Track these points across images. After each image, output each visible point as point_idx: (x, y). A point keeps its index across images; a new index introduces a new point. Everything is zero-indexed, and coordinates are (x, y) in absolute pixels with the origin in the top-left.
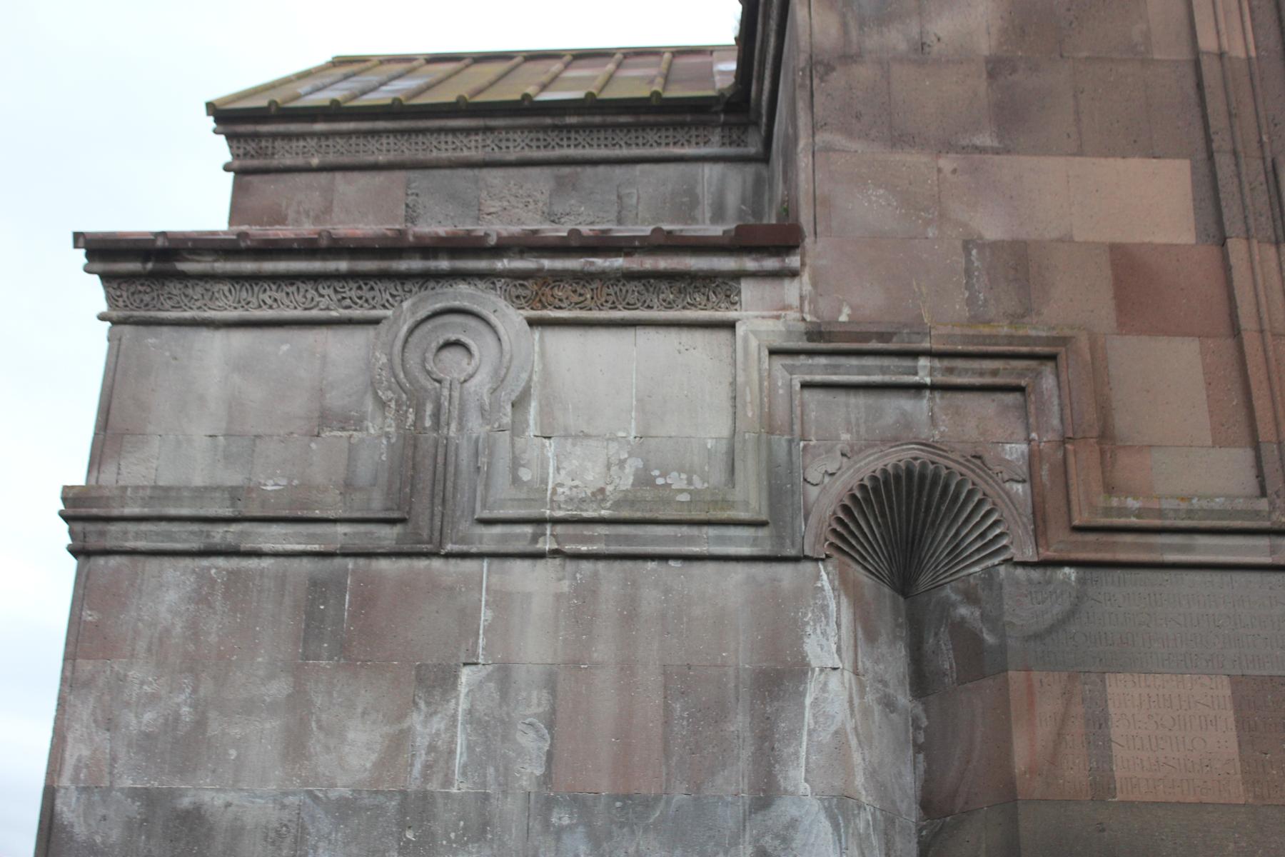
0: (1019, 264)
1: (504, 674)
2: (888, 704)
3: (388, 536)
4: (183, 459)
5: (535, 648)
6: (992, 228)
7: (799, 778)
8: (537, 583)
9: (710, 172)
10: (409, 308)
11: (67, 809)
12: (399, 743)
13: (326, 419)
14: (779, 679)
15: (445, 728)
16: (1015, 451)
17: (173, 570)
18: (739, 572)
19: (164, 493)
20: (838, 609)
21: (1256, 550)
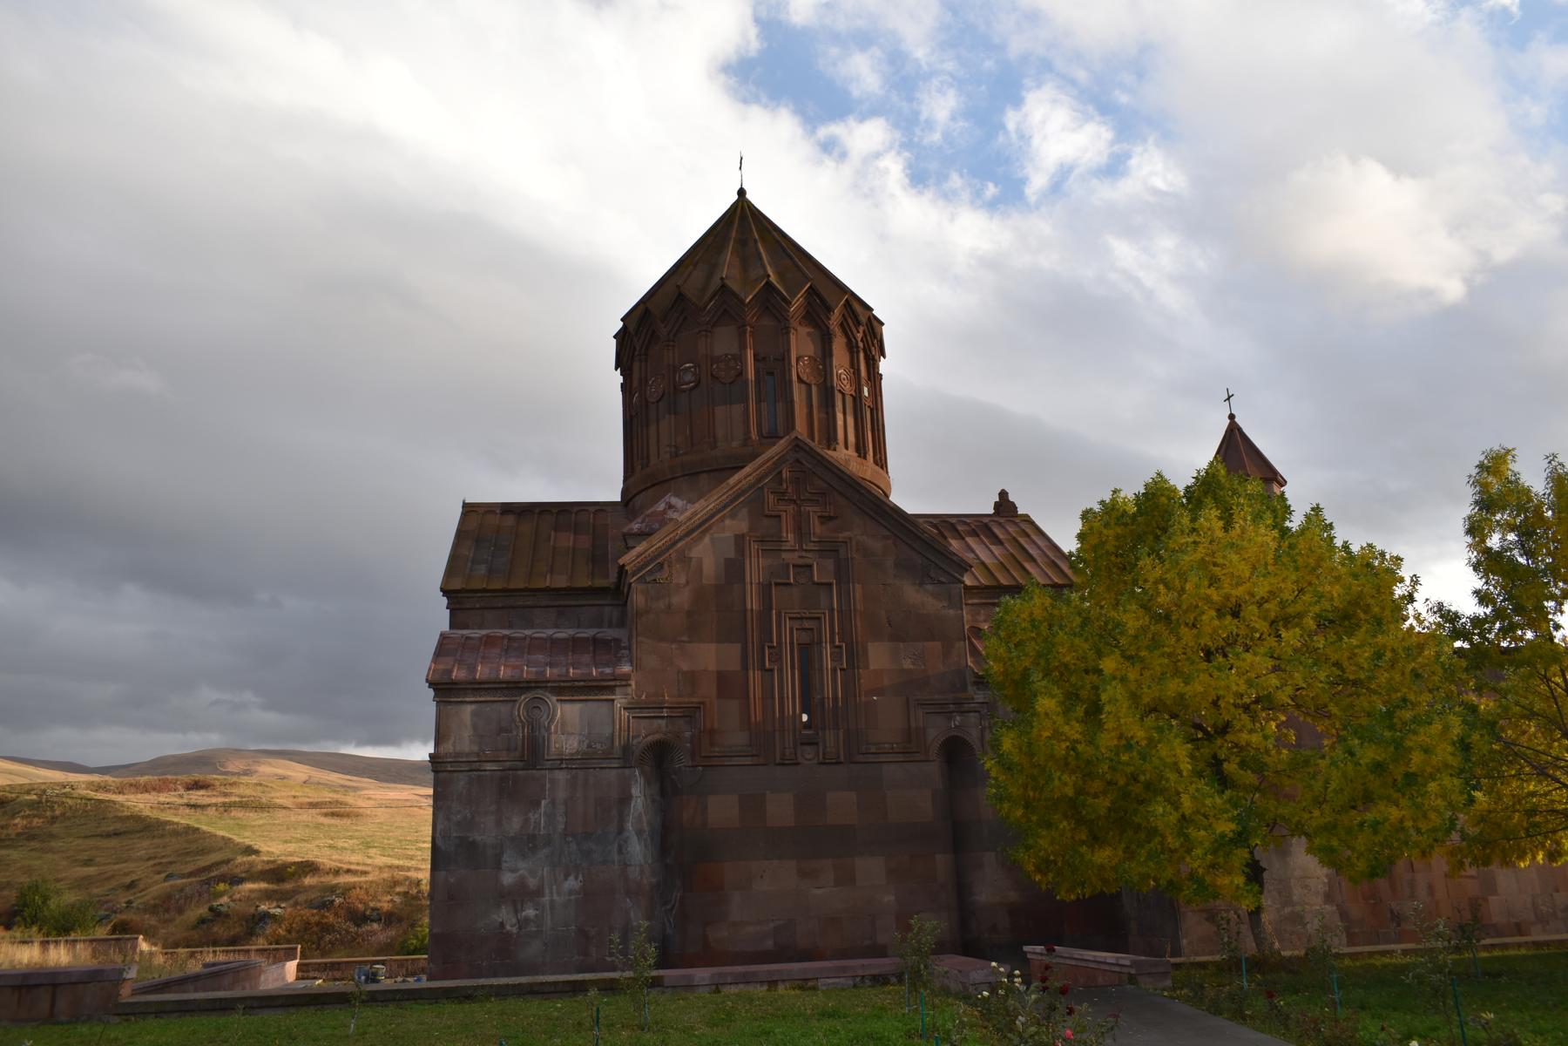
0: (692, 678)
1: (553, 802)
2: (653, 801)
3: (520, 764)
4: (463, 742)
5: (561, 795)
6: (685, 667)
7: (629, 826)
8: (561, 776)
9: (607, 609)
10: (523, 699)
11: (439, 842)
12: (526, 821)
13: (501, 730)
14: (625, 799)
15: (539, 817)
16: (688, 734)
17: (461, 776)
18: (614, 772)
19: (458, 754)
20: (641, 780)
21: (748, 761)
